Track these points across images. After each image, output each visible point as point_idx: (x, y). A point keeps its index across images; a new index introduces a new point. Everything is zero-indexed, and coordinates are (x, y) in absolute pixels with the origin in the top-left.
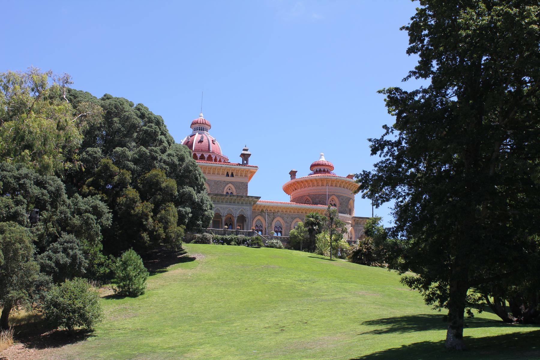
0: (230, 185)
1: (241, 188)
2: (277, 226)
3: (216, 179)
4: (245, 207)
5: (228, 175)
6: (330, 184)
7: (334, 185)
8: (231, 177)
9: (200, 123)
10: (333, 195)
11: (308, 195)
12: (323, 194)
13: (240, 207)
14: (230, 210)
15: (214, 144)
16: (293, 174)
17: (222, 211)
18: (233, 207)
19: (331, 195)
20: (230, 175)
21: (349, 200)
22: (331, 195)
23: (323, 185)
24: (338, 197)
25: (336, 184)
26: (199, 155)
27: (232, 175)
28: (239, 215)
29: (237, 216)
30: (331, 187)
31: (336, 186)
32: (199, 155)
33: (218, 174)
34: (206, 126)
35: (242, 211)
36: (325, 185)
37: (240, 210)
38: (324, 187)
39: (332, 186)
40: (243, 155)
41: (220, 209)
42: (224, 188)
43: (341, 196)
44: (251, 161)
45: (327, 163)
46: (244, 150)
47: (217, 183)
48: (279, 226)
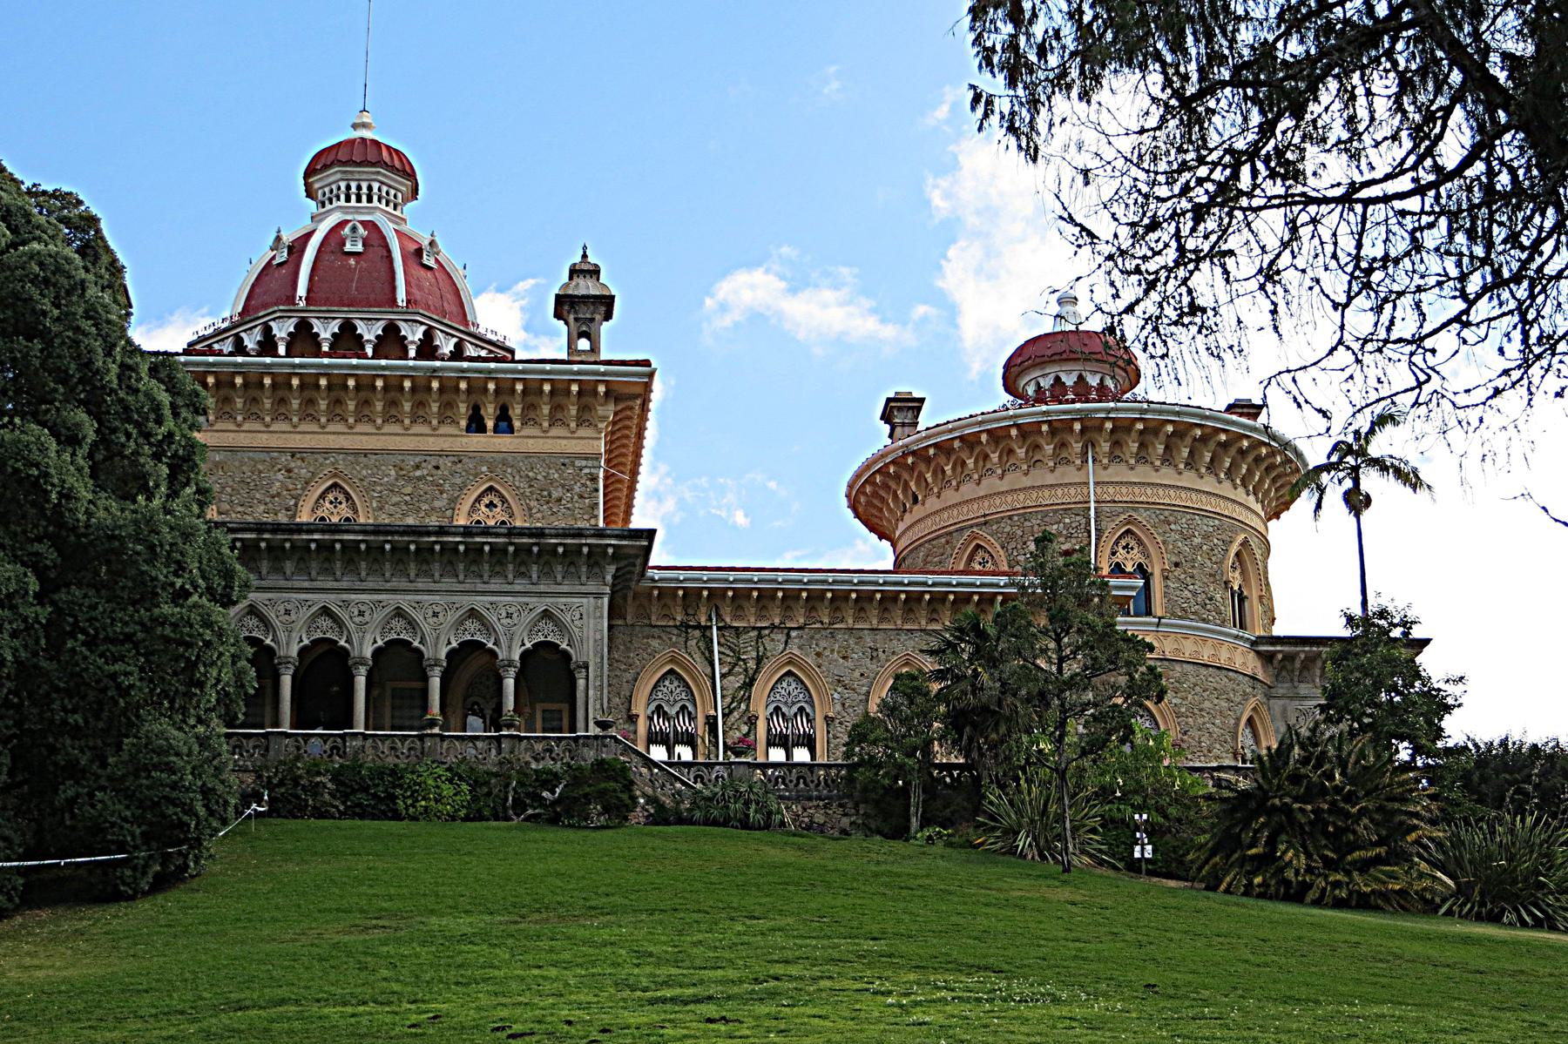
1: (555, 495)
2: (784, 709)
8: (496, 430)
16: (900, 410)
26: (325, 331)
32: (325, 331)
38: (1070, 474)
42: (453, 502)
44: (615, 341)
48: (795, 709)
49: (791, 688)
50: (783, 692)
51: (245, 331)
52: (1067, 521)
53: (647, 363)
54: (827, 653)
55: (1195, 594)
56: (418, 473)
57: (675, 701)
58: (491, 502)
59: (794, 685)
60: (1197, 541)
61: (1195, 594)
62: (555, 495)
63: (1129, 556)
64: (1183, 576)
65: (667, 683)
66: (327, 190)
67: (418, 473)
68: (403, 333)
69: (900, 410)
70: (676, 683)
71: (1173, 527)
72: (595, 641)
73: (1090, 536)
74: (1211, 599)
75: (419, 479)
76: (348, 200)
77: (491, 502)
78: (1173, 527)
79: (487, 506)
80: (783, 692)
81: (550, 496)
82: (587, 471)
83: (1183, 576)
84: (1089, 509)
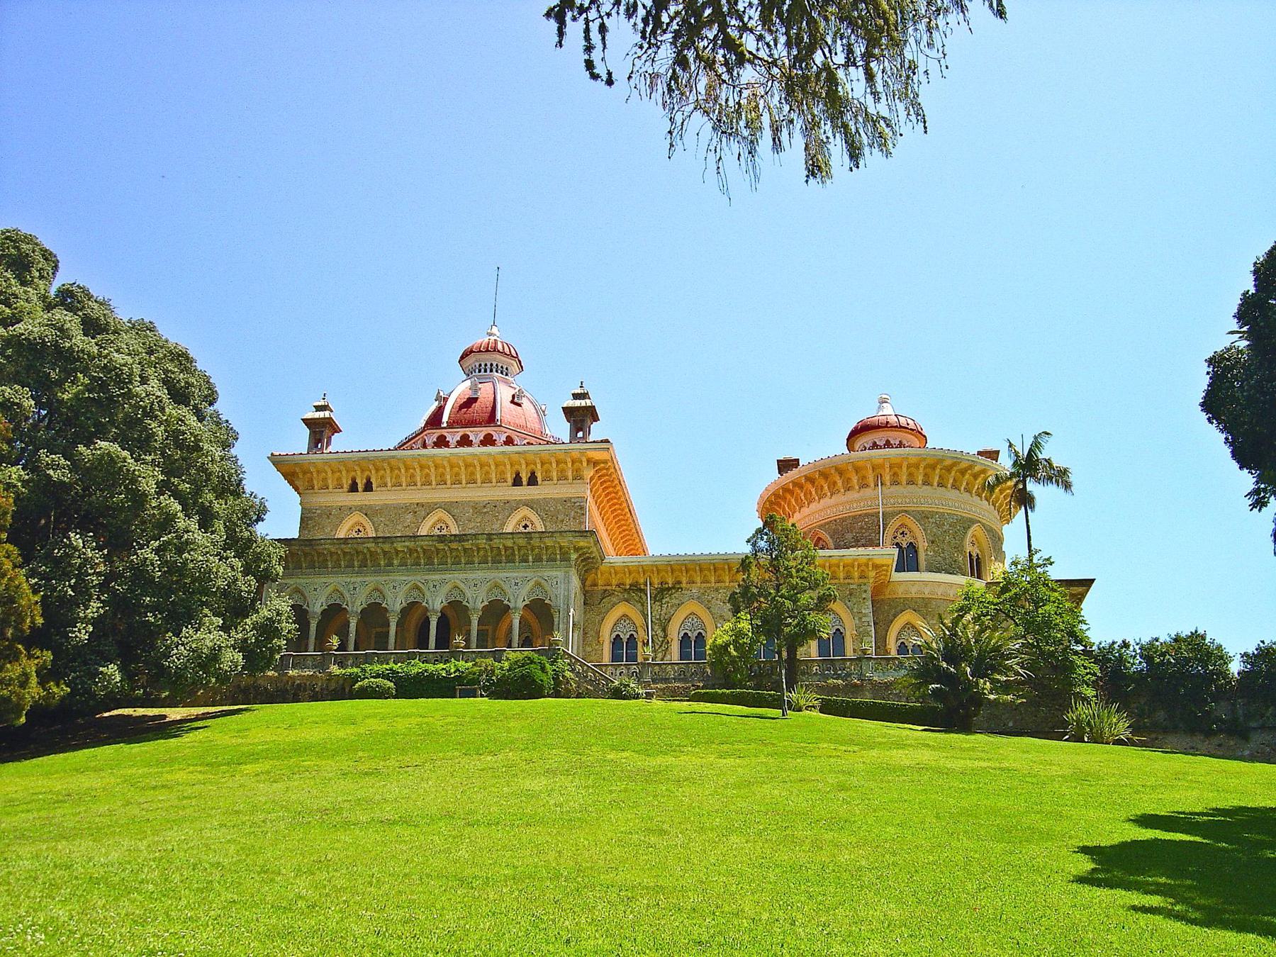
0: (525, 511)
1: (560, 518)
3: (480, 499)
4: (547, 573)
5: (517, 482)
6: (887, 478)
7: (904, 478)
9: (480, 351)
10: (903, 511)
11: (820, 527)
12: (867, 515)
13: (529, 574)
14: (496, 586)
15: (519, 405)
17: (468, 594)
18: (508, 575)
19: (894, 514)
20: (525, 480)
21: (967, 529)
22: (894, 514)
23: (864, 485)
24: (923, 517)
25: (910, 474)
27: (533, 481)
28: (527, 602)
29: (521, 605)
30: (894, 488)
31: (911, 482)
33: (487, 480)
34: (498, 356)
35: (538, 584)
36: (872, 485)
37: (532, 583)
38: (868, 492)
39: (895, 482)
40: (568, 412)
41: (462, 586)
43: (933, 514)
45: (893, 420)
46: (576, 396)
47: (479, 509)
49: (693, 622)
50: (689, 624)
51: (414, 443)
52: (866, 520)
53: (607, 441)
54: (714, 600)
55: (945, 559)
56: (485, 510)
57: (627, 632)
58: (526, 524)
59: (696, 620)
60: (946, 527)
61: (945, 559)
62: (560, 518)
63: (904, 539)
64: (936, 549)
65: (622, 622)
66: (470, 368)
67: (485, 510)
68: (494, 438)
69: (786, 465)
70: (628, 622)
71: (930, 520)
72: (564, 596)
73: (880, 528)
74: (955, 561)
75: (485, 513)
76: (480, 371)
77: (526, 524)
78: (930, 520)
79: (523, 527)
80: (689, 624)
81: (557, 518)
82: (578, 504)
83: (936, 549)
84: (879, 513)
